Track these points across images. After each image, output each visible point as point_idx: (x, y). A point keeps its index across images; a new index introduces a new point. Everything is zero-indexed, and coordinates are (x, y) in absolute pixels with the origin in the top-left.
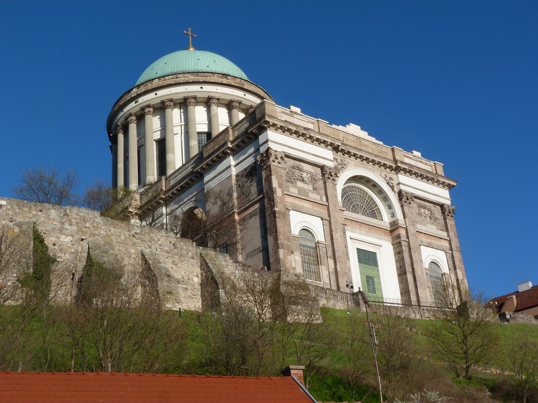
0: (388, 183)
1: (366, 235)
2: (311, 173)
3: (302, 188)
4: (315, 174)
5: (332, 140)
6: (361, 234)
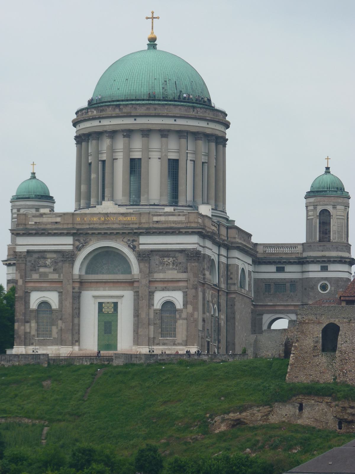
0: (129, 246)
1: (109, 290)
2: (54, 258)
3: (43, 272)
4: (56, 258)
5: (67, 231)
6: (104, 290)
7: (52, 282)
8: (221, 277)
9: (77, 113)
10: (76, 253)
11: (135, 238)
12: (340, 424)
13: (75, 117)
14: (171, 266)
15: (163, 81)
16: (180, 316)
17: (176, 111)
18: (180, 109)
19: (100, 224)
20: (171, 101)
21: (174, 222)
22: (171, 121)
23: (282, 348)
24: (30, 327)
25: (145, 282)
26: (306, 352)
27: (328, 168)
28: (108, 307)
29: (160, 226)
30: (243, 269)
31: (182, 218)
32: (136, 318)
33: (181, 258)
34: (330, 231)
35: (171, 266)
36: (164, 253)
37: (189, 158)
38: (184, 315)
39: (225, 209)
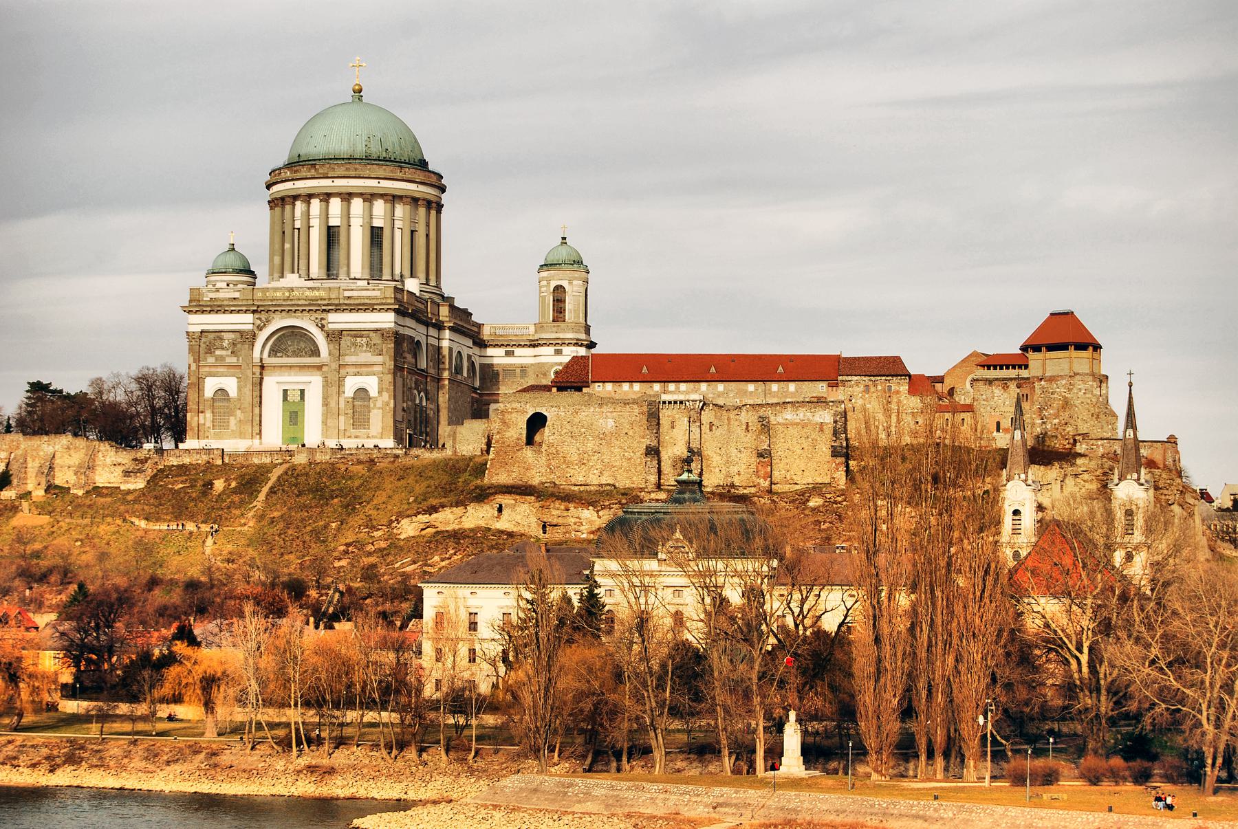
0: (317, 325)
1: (295, 375)
6: (289, 375)
7: (230, 366)
8: (429, 360)
9: (270, 174)
10: (257, 332)
11: (324, 315)
12: (544, 527)
13: (269, 178)
14: (364, 348)
15: (366, 138)
16: (375, 405)
17: (381, 172)
18: (385, 169)
19: (284, 300)
20: (375, 160)
21: (369, 298)
22: (373, 183)
23: (485, 441)
24: (205, 418)
25: (334, 366)
26: (509, 446)
27: (564, 238)
28: (294, 395)
29: (352, 302)
30: (459, 352)
31: (377, 293)
32: (325, 408)
33: (376, 339)
34: (565, 310)
35: (364, 348)
36: (357, 333)
37: (396, 226)
38: (379, 404)
39: (440, 283)
